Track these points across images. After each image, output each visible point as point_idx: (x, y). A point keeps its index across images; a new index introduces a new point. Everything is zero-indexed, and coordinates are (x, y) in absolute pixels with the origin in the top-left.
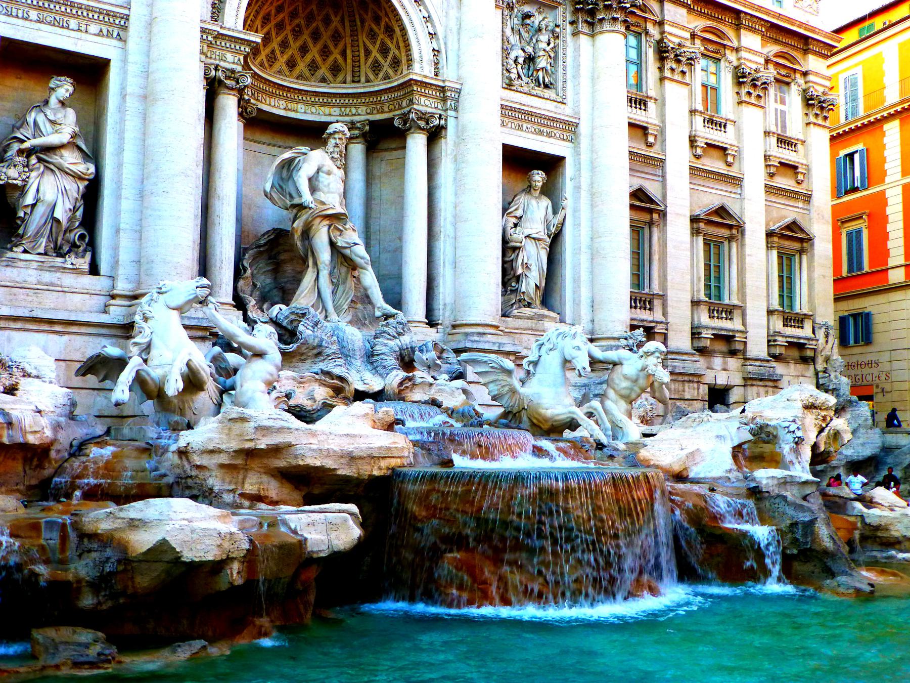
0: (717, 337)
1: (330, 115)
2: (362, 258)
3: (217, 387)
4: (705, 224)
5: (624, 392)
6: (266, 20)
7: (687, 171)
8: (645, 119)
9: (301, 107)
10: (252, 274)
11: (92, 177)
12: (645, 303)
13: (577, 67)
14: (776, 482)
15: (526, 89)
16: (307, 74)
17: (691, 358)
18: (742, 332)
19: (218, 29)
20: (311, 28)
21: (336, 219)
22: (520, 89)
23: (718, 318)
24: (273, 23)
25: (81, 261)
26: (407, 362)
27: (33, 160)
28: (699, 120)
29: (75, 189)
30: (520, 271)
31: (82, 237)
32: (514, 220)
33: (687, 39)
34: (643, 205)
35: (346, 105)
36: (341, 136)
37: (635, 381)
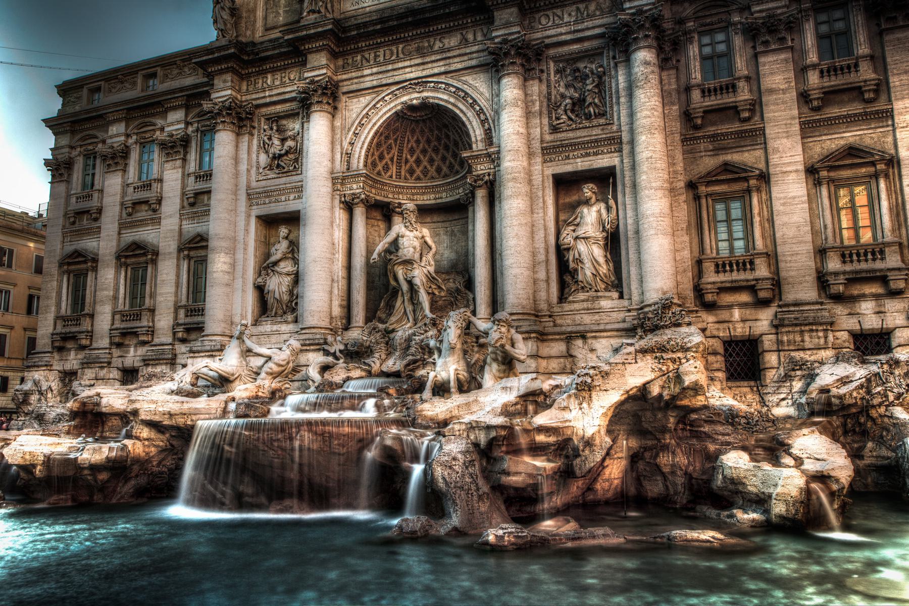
0: (856, 279)
4: (828, 171)
6: (412, 151)
7: (797, 128)
8: (733, 99)
12: (744, 264)
13: (617, 92)
14: (464, 427)
15: (574, 126)
18: (899, 269)
23: (859, 261)
24: (418, 152)
29: (287, 280)
30: (572, 265)
32: (572, 228)
34: (730, 176)
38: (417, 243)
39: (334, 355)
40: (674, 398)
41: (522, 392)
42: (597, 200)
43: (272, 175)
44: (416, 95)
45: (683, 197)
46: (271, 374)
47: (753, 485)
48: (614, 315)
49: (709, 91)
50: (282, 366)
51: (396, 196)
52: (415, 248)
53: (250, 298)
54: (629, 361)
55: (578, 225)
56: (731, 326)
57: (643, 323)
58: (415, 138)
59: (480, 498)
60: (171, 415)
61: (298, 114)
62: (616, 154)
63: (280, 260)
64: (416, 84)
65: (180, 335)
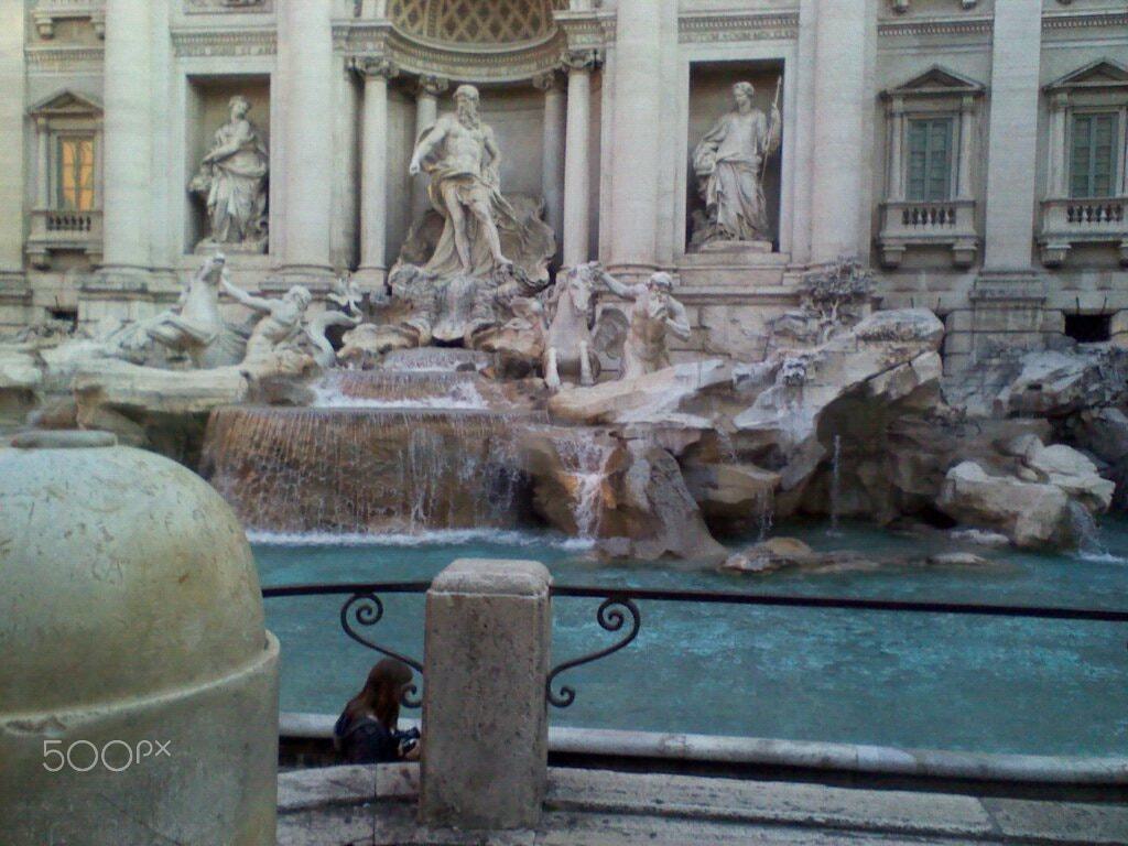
1: (530, 71)
2: (480, 213)
3: (235, 341)
7: (1039, 23)
9: (503, 70)
11: (262, 174)
12: (942, 215)
14: (649, 428)
17: (1030, 277)
21: (463, 178)
23: (1089, 220)
26: (503, 308)
27: (215, 169)
29: (248, 187)
30: (710, 200)
34: (939, 89)
38: (477, 148)
39: (346, 309)
40: (903, 398)
41: (704, 384)
42: (752, 107)
45: (871, 113)
47: (994, 504)
48: (766, 274)
50: (288, 325)
51: (428, 65)
52: (474, 156)
53: (181, 210)
54: (849, 350)
55: (721, 141)
56: (915, 298)
57: (814, 290)
59: (689, 516)
62: (785, 42)
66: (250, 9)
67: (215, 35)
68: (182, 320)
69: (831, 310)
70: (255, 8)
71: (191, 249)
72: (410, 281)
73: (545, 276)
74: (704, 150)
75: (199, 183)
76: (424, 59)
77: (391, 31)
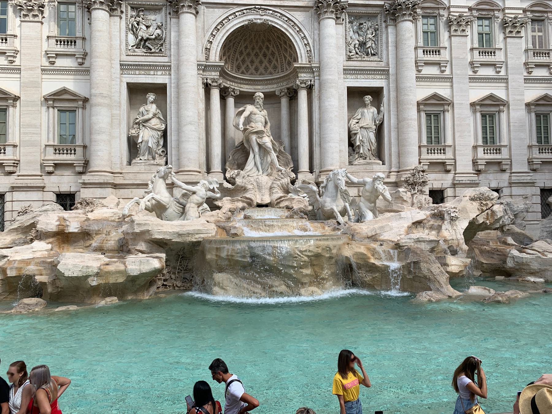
0: (489, 163)
5: (368, 198)
6: (241, 53)
7: (468, 80)
8: (439, 59)
10: (234, 159)
11: (163, 129)
12: (440, 151)
13: (387, 43)
15: (359, 59)
16: (264, 72)
17: (473, 175)
19: (205, 63)
20: (262, 53)
22: (355, 59)
23: (490, 153)
24: (245, 54)
25: (160, 161)
27: (141, 126)
28: (476, 52)
30: (358, 143)
31: (163, 151)
33: (466, 12)
35: (278, 83)
36: (258, 98)
37: (371, 192)
38: (263, 120)
40: (491, 224)
43: (139, 51)
44: (259, 17)
46: (197, 204)
49: (427, 52)
51: (231, 83)
52: (262, 123)
58: (245, 45)
60: (180, 235)
61: (160, 10)
62: (384, 80)
63: (150, 119)
64: (259, 9)
65: (51, 169)
66: (157, 55)
67: (142, 65)
68: (158, 197)
69: (414, 189)
70: (159, 54)
71: (130, 163)
72: (243, 177)
73: (295, 176)
74: (354, 123)
75: (133, 132)
76: (230, 81)
77: (222, 67)
